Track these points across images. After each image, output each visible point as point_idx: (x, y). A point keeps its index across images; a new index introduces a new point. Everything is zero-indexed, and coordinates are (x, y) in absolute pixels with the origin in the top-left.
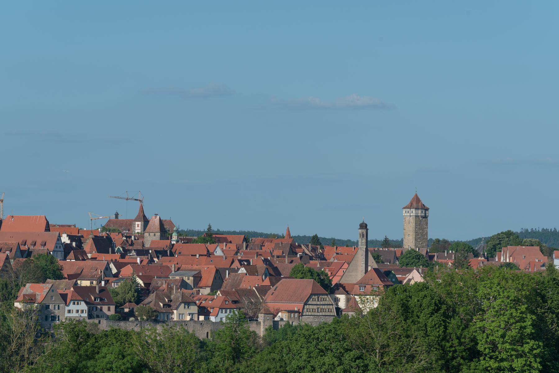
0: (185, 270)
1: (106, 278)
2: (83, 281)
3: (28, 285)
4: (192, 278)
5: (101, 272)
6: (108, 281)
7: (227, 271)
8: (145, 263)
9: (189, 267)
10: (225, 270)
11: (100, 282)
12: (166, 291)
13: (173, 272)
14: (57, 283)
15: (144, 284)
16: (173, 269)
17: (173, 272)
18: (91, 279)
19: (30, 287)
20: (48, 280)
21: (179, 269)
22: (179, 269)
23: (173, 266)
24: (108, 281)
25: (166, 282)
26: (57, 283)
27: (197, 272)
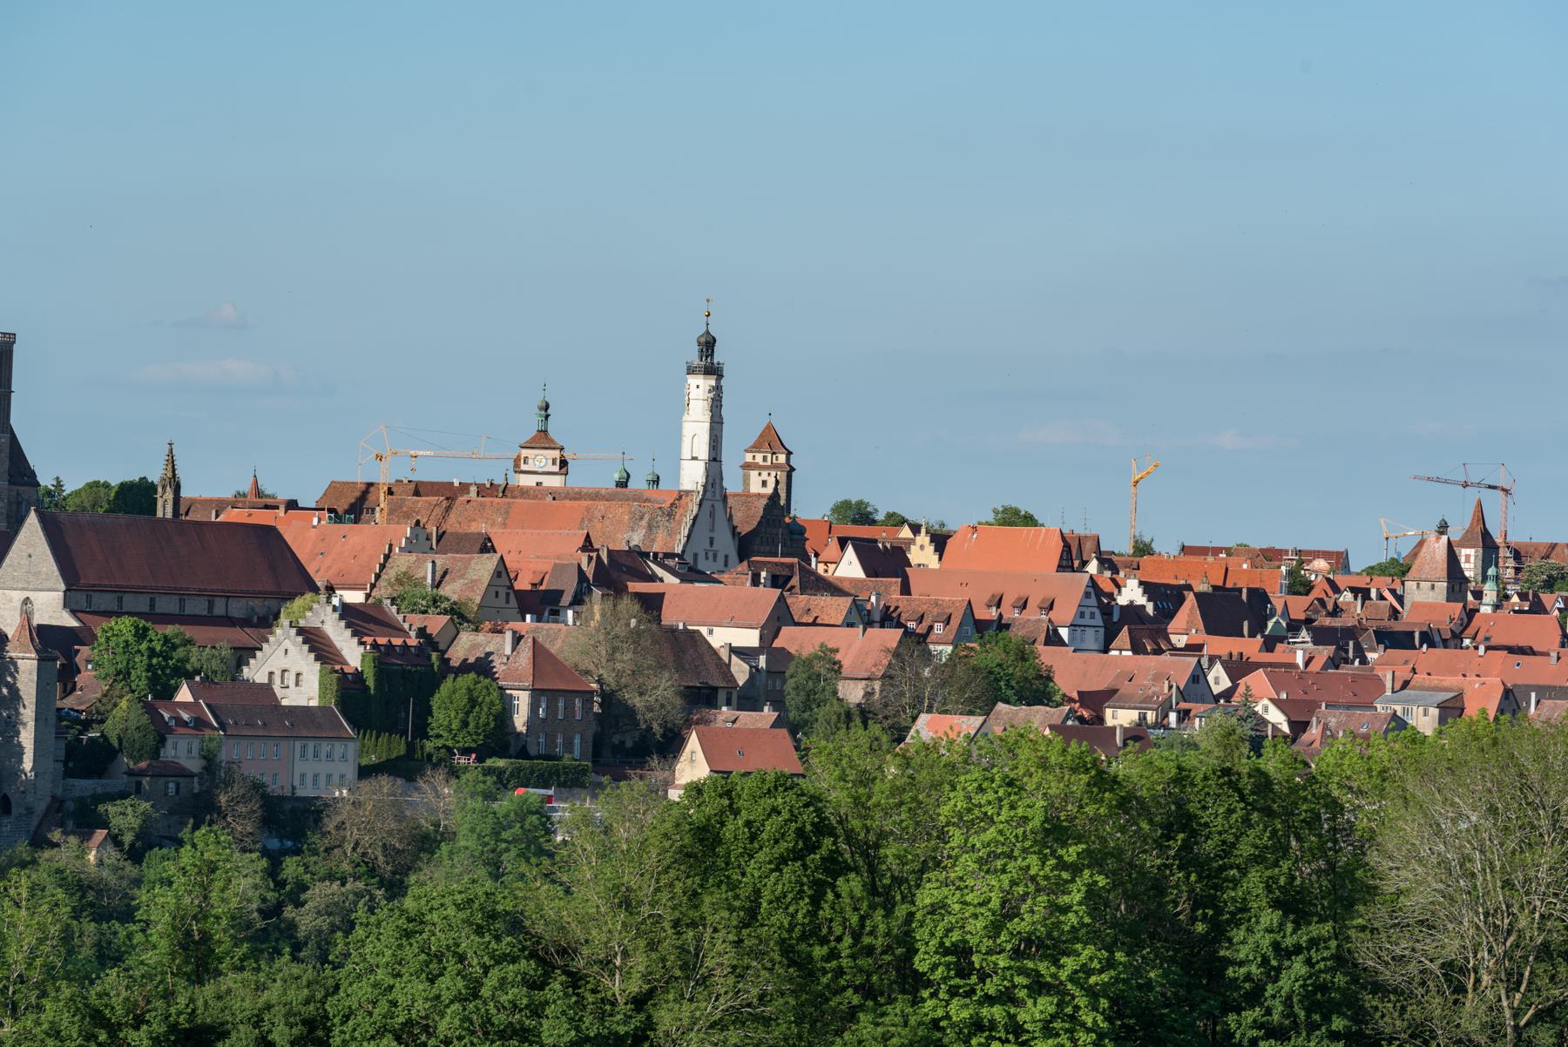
0: (1422, 688)
1: (1183, 705)
2: (1120, 711)
3: (924, 718)
4: (1434, 712)
5: (1170, 687)
6: (1187, 712)
7: (1533, 695)
8: (1316, 666)
9: (1435, 680)
10: (1529, 688)
11: (1167, 716)
12: (1317, 744)
13: (1389, 693)
14: (1021, 714)
15: (1291, 723)
16: (1389, 685)
17: (1389, 693)
18: (1142, 704)
19: (928, 724)
20: (1001, 706)
21: (1405, 685)
22: (1405, 685)
23: (1389, 676)
24: (1187, 712)
25: (1319, 722)
26: (1021, 714)
27: (1452, 695)
